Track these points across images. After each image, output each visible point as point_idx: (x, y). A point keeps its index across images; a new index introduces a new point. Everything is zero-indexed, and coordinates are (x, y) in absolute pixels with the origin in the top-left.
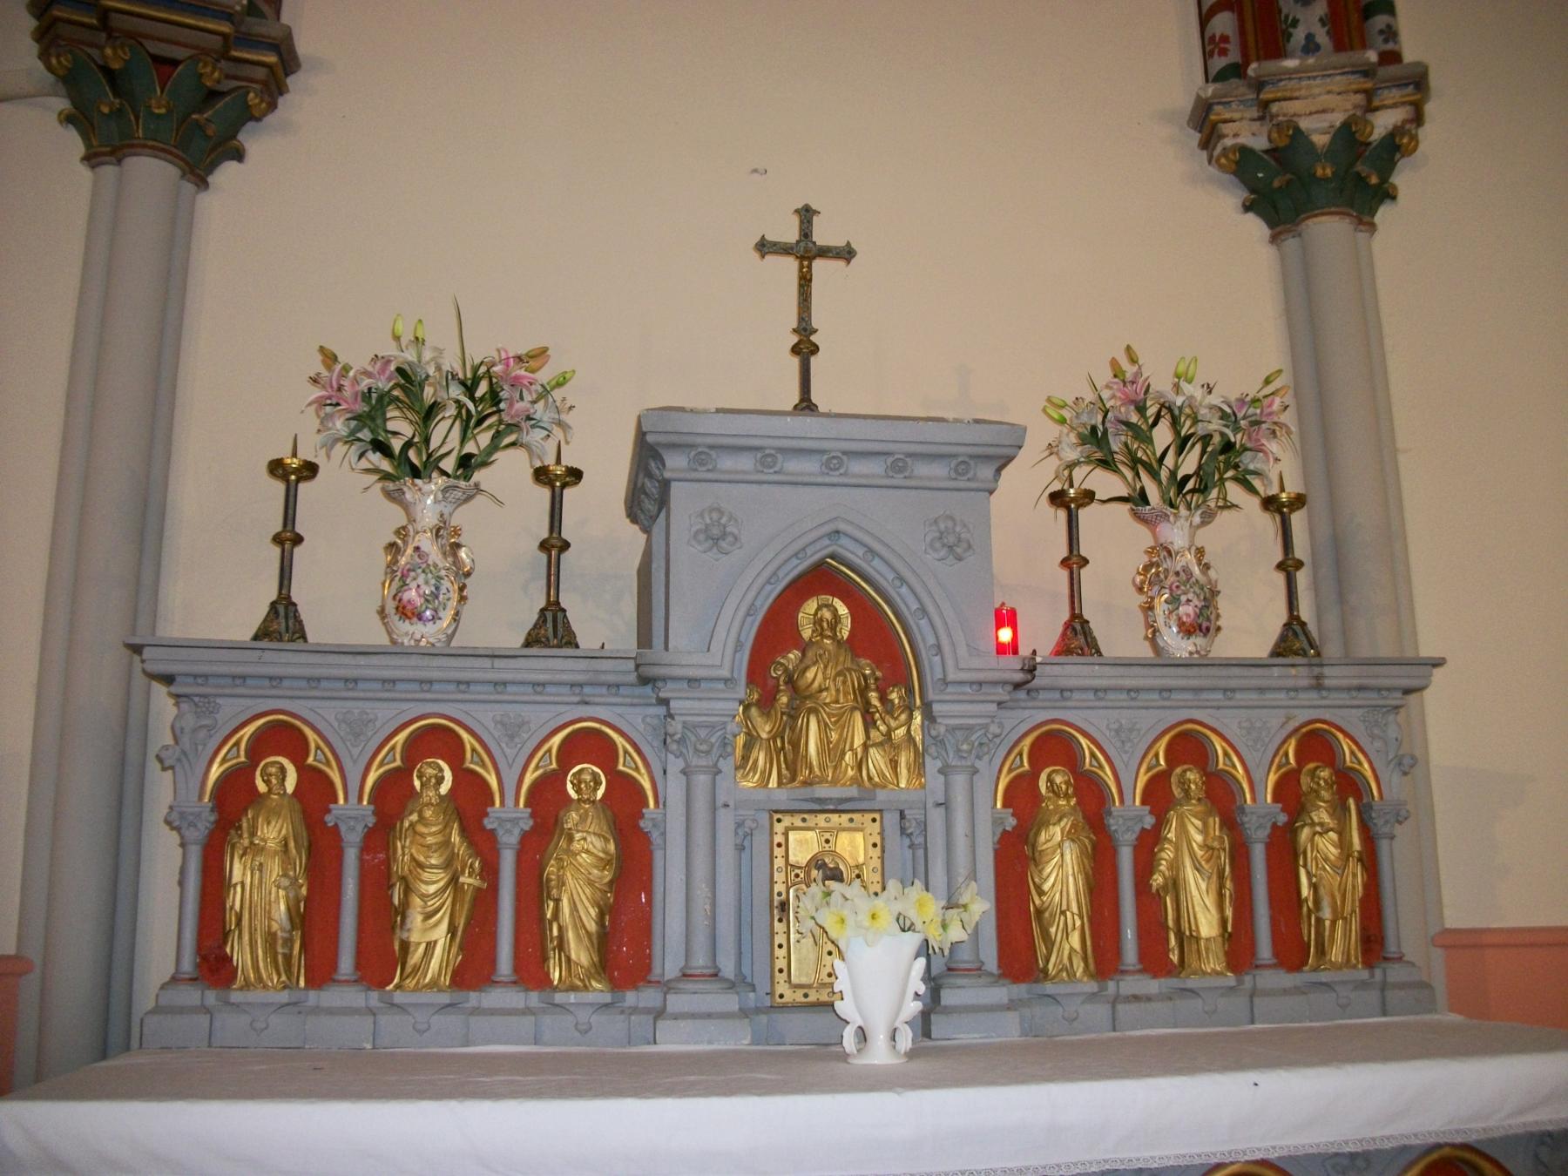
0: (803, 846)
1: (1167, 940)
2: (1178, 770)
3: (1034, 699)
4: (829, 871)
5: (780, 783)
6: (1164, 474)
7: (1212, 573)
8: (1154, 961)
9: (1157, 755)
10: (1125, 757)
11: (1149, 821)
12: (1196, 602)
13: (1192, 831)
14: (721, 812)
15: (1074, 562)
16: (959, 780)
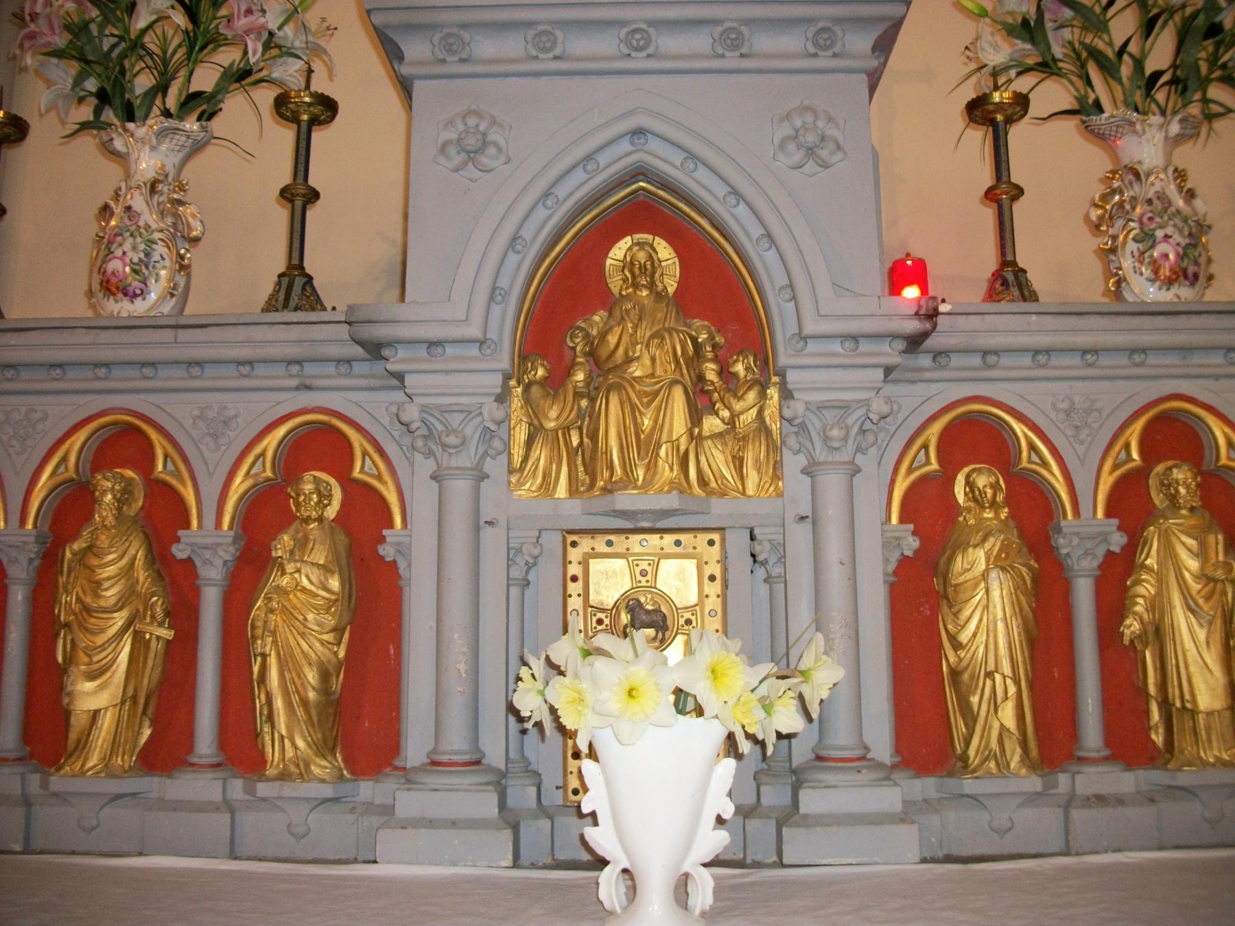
0: (610, 580)
1: (1147, 713)
2: (1160, 468)
3: (942, 367)
4: (647, 618)
5: (573, 491)
6: (1126, 70)
7: (1198, 203)
8: (1128, 745)
9: (1127, 446)
10: (1081, 449)
11: (1118, 541)
12: (1177, 238)
13: (1183, 555)
14: (487, 532)
15: (1003, 194)
16: (833, 482)
